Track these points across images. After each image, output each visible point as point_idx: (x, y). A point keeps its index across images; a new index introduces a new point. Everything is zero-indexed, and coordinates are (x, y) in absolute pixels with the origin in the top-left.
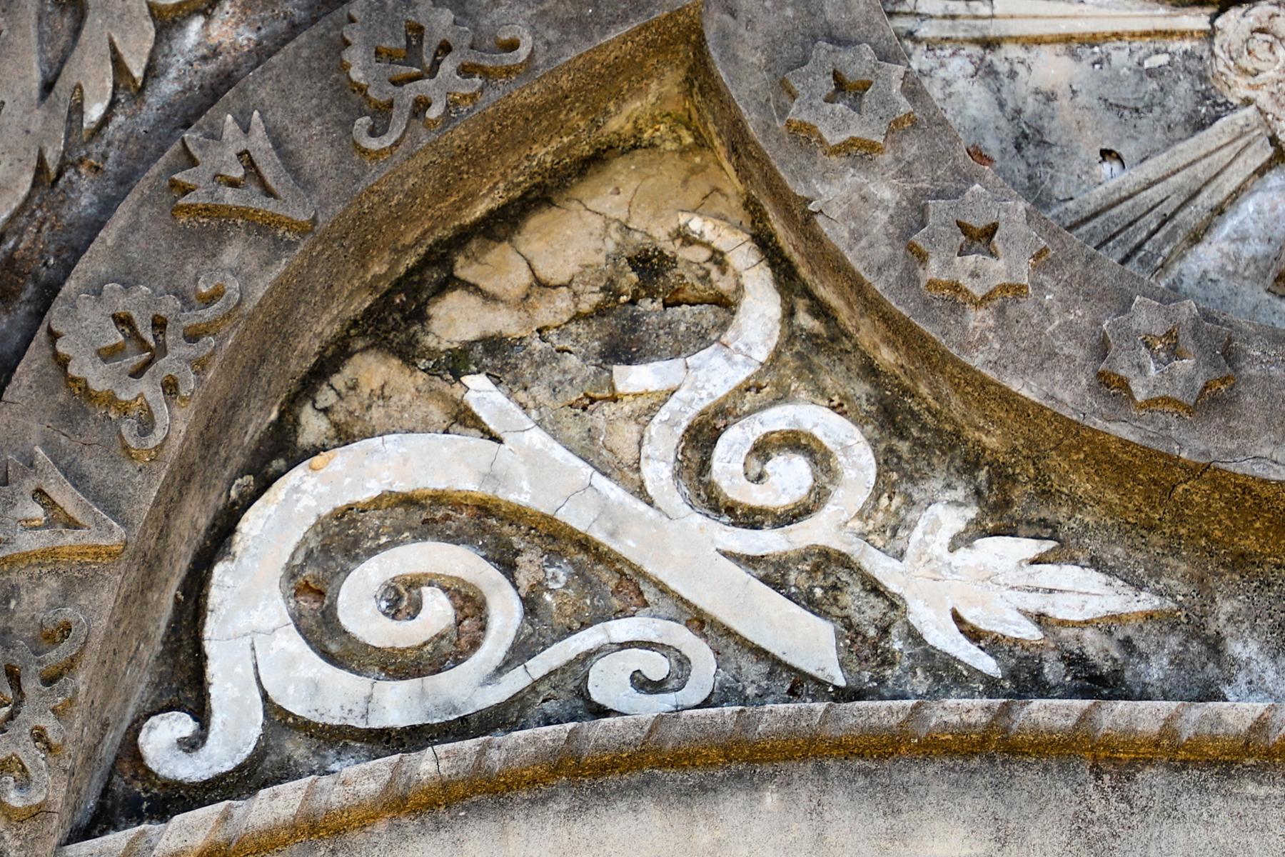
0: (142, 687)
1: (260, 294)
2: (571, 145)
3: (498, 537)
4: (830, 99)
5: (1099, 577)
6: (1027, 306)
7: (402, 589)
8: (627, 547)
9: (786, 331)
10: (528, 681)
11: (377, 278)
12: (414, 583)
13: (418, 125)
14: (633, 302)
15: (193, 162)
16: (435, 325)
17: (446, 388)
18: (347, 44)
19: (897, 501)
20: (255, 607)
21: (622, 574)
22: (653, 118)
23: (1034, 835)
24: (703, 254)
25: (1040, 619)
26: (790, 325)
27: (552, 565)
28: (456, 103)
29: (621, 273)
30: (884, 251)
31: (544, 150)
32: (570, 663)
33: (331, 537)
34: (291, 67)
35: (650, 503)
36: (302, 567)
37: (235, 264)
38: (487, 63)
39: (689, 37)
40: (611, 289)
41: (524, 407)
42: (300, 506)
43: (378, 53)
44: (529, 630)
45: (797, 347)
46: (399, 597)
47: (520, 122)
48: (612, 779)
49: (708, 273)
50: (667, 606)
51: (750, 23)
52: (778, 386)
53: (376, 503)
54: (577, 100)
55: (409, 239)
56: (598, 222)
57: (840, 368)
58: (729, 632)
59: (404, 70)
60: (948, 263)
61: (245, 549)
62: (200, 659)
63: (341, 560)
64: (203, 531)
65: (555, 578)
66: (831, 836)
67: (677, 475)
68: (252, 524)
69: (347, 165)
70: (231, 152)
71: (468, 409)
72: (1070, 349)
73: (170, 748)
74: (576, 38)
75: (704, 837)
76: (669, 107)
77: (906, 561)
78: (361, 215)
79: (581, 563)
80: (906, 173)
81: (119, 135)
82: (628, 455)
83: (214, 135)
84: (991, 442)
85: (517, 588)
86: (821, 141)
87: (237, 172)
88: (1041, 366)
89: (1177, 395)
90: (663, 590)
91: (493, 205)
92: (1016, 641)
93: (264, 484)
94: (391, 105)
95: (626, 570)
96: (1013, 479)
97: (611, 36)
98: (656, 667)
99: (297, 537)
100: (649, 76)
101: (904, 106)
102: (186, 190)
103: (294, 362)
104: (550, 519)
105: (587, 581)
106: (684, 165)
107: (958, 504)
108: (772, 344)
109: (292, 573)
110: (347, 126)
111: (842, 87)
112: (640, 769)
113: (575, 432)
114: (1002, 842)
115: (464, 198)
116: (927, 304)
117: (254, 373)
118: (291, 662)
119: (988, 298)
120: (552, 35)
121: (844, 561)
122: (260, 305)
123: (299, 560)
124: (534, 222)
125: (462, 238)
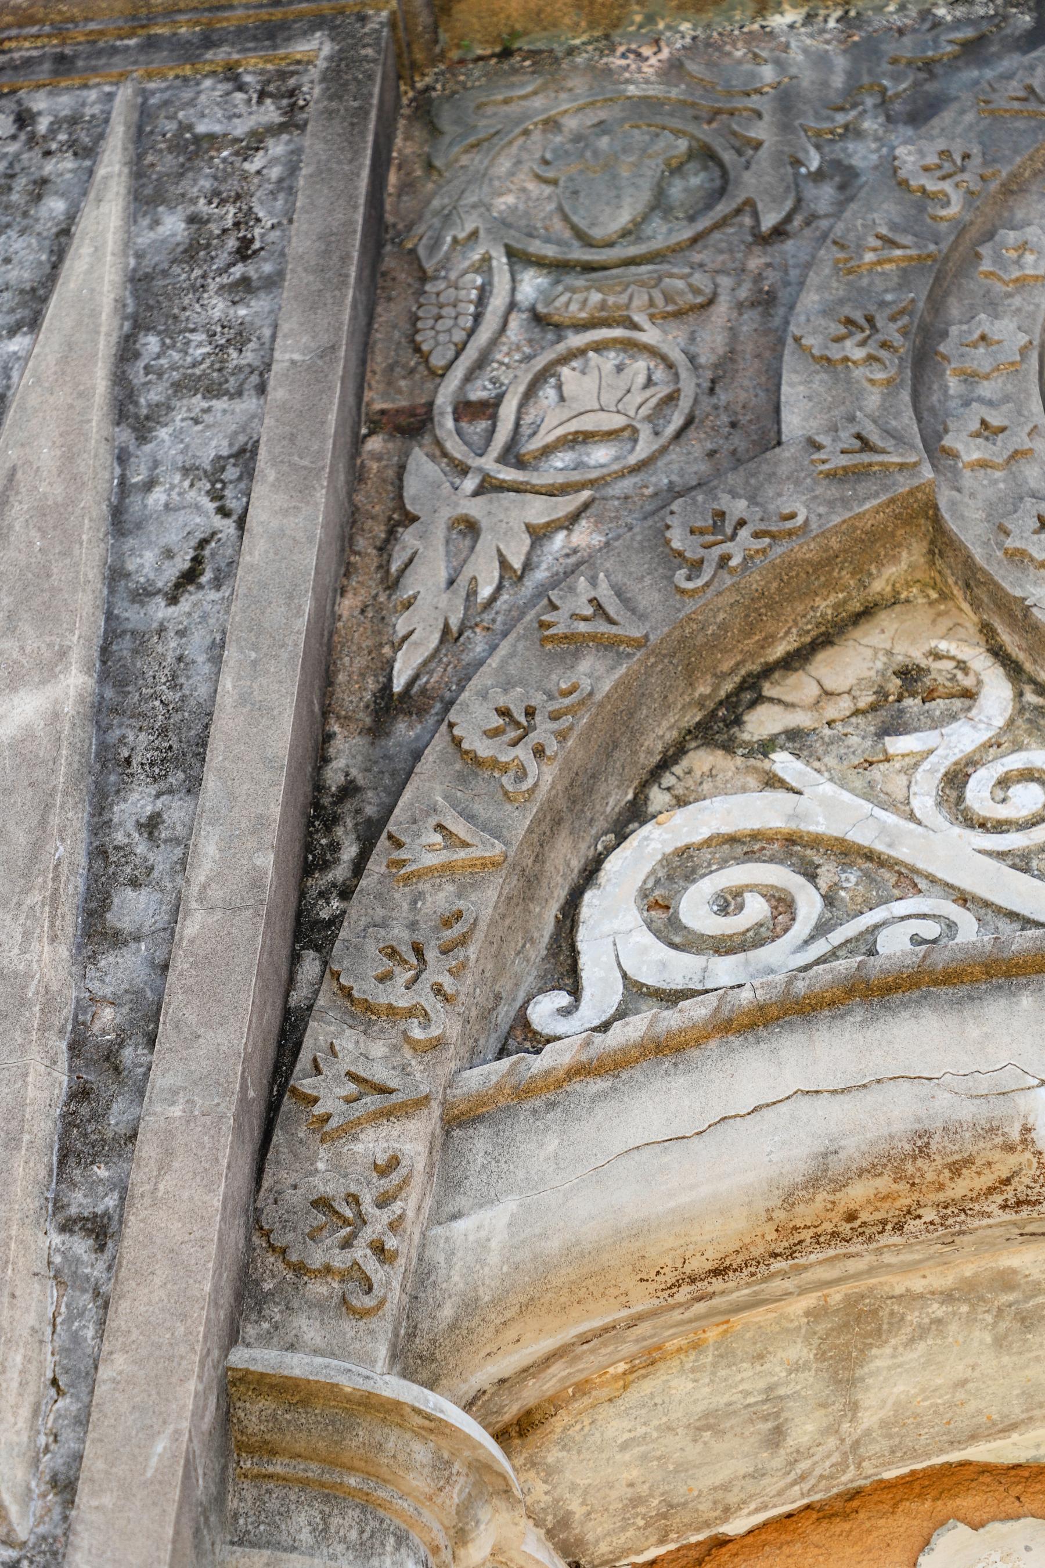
0: (530, 979)
1: (607, 688)
2: (845, 602)
3: (802, 858)
4: (1035, 532)
7: (729, 898)
8: (903, 853)
9: (1018, 706)
10: (829, 948)
11: (703, 697)
12: (738, 893)
13: (724, 574)
14: (899, 700)
15: (555, 608)
16: (750, 726)
17: (758, 764)
18: (668, 527)
21: (900, 874)
22: (907, 582)
24: (953, 664)
26: (1020, 702)
27: (845, 872)
28: (751, 557)
29: (888, 680)
31: (824, 604)
32: (862, 934)
33: (675, 869)
34: (628, 548)
35: (920, 823)
36: (653, 890)
37: (588, 671)
38: (773, 528)
39: (927, 513)
40: (882, 693)
41: (818, 771)
42: (649, 849)
43: (692, 532)
44: (828, 915)
45: (1027, 715)
46: (728, 905)
47: (803, 575)
49: (955, 676)
50: (937, 889)
51: (972, 495)
52: (1014, 742)
53: (708, 842)
54: (845, 560)
55: (726, 666)
58: (987, 904)
59: (710, 538)
61: (608, 880)
62: (574, 953)
63: (681, 883)
64: (576, 871)
65: (847, 880)
67: (939, 804)
68: (612, 865)
69: (671, 602)
70: (584, 599)
71: (775, 775)
73: (551, 1015)
74: (840, 510)
75: (974, 1032)
76: (919, 575)
78: (683, 640)
79: (868, 869)
81: (505, 607)
82: (900, 795)
83: (572, 589)
85: (818, 889)
86: (1032, 559)
87: (589, 611)
90: (933, 880)
93: (622, 837)
94: (702, 561)
95: (903, 870)
97: (867, 506)
98: (930, 930)
99: (648, 868)
100: (900, 545)
102: (550, 626)
103: (642, 755)
104: (841, 841)
105: (873, 880)
106: (932, 612)
108: (1007, 715)
110: (670, 578)
112: (919, 988)
113: (859, 784)
115: (765, 639)
117: (609, 755)
118: (644, 950)
120: (822, 510)
122: (607, 696)
123: (649, 885)
124: (821, 656)
125: (768, 671)
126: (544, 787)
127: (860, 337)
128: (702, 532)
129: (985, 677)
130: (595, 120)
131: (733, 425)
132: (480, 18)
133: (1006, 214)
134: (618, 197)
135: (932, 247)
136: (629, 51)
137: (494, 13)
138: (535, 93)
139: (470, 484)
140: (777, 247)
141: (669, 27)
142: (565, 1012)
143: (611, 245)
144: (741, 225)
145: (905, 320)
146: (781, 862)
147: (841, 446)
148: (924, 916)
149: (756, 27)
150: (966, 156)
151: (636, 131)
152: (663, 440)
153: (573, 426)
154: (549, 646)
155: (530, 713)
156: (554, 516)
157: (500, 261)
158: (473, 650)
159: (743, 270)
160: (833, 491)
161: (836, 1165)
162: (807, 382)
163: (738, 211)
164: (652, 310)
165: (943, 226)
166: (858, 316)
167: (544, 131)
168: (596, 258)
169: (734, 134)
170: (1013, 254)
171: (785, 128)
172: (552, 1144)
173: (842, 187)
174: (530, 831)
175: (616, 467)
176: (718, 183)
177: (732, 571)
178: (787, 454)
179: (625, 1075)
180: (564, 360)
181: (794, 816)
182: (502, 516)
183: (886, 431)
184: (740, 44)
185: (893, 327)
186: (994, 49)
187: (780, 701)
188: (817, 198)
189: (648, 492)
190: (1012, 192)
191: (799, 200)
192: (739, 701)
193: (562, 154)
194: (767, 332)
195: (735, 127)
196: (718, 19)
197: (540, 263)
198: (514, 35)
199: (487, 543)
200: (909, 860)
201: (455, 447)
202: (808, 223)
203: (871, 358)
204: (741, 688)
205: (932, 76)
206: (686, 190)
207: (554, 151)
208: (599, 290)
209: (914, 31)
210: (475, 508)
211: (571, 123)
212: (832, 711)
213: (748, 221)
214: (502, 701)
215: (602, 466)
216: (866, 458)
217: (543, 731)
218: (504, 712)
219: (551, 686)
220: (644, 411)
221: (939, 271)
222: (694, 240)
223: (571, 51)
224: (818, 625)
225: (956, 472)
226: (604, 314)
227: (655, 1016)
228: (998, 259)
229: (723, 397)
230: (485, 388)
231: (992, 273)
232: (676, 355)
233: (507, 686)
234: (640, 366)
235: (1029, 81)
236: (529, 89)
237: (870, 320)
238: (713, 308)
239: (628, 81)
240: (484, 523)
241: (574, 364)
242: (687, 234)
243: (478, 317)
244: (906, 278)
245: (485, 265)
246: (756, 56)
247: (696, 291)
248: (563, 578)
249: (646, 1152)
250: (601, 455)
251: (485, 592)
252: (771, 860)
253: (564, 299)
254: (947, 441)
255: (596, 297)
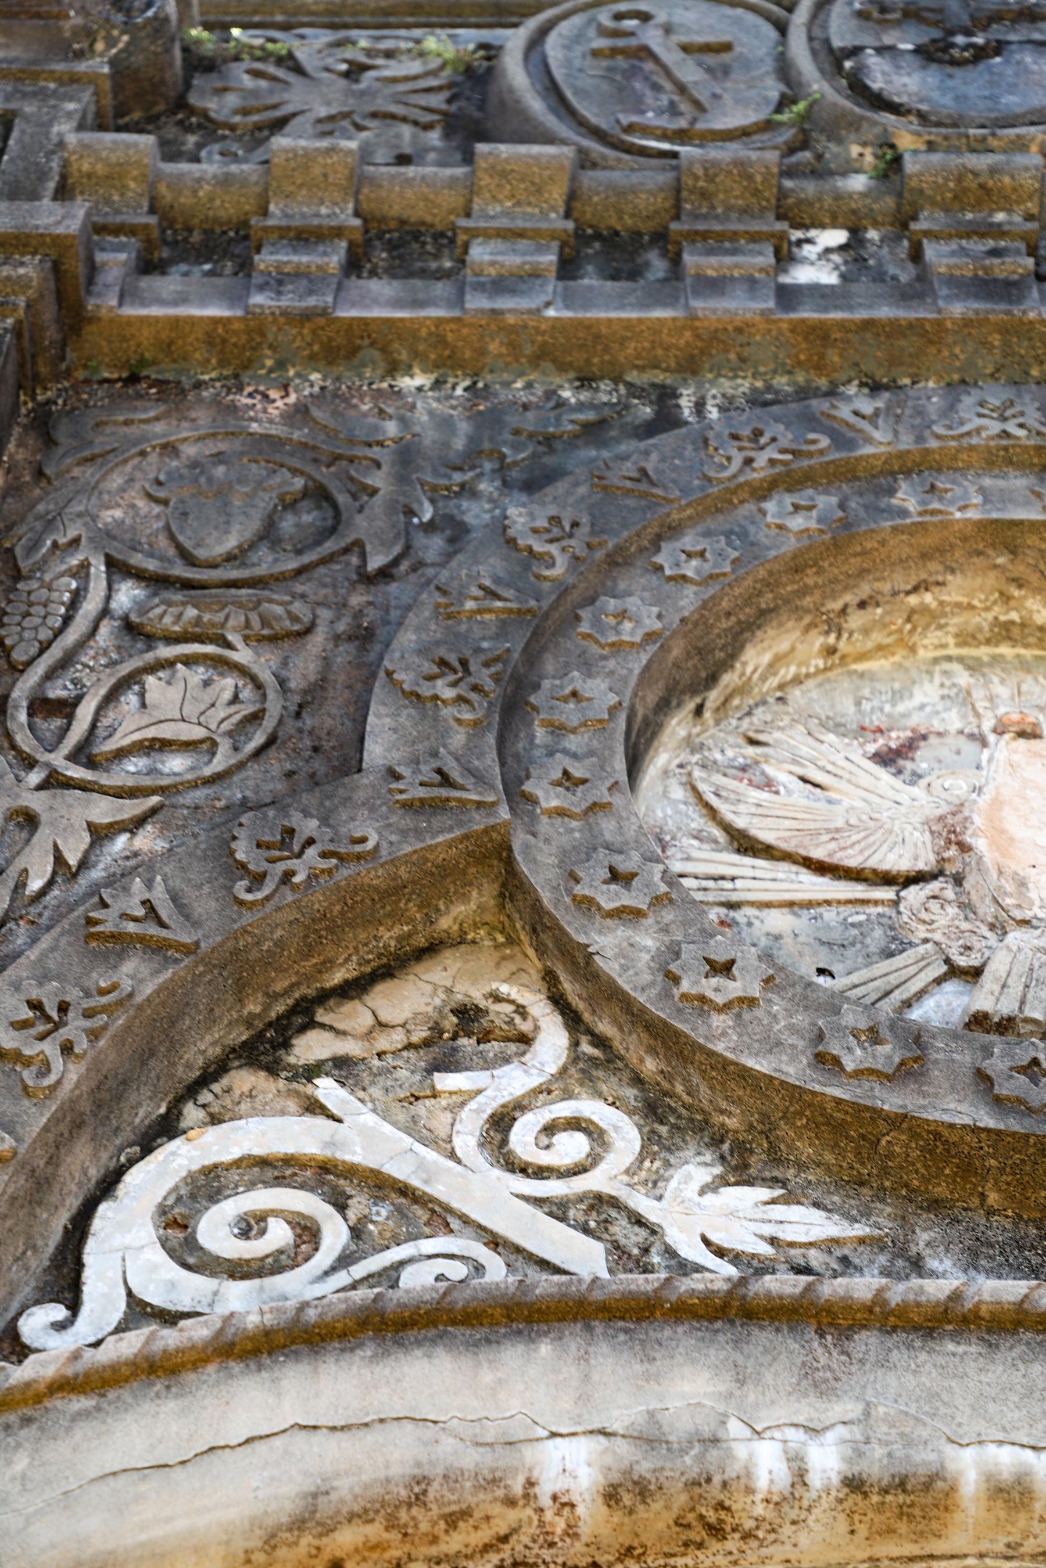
0: (28, 1289)
1: (149, 991)
2: (410, 935)
3: (334, 1188)
4: (605, 882)
5: (823, 1214)
6: (759, 1013)
8: (438, 1190)
13: (286, 890)
15: (104, 905)
16: (296, 1051)
17: (300, 1088)
18: (234, 838)
19: (657, 1164)
20: (129, 1231)
21: (433, 1211)
23: (769, 1377)
25: (773, 1241)
28: (316, 876)
29: (445, 1017)
30: (647, 977)
31: (388, 935)
32: (386, 1269)
33: (199, 1188)
35: (459, 1162)
40: (437, 1029)
41: (361, 1101)
42: (175, 1165)
44: (354, 1247)
45: (581, 1065)
46: (250, 1228)
47: (368, 902)
48: (412, 1334)
50: (469, 1231)
51: (547, 841)
53: (237, 1163)
55: (279, 986)
56: (429, 988)
57: (614, 1080)
58: (518, 1250)
59: (277, 853)
60: (696, 983)
62: (79, 1266)
64: (93, 1181)
65: (378, 1214)
66: (596, 1377)
67: (481, 1145)
68: (133, 1178)
69: (228, 912)
70: (136, 900)
71: (317, 1101)
72: (793, 1040)
73: (45, 1328)
75: (487, 1377)
76: (488, 917)
77: (664, 1201)
78: (236, 952)
80: (665, 930)
82: (443, 1133)
83: (126, 889)
84: (732, 1123)
85: (346, 1220)
86: (599, 908)
87: (140, 912)
88: (770, 1051)
89: (879, 1067)
90: (466, 1220)
91: (348, 976)
92: (753, 1256)
93: (147, 1150)
94: (264, 875)
96: (751, 1151)
97: (440, 839)
98: (457, 1271)
99: (170, 1184)
100: (471, 884)
101: (663, 888)
103: (181, 1069)
104: (376, 1173)
106: (497, 955)
107: (706, 1164)
109: (163, 1210)
110: (229, 889)
111: (615, 876)
112: (436, 1326)
114: (741, 1382)
115: (324, 963)
116: (679, 1011)
117: (144, 1063)
118: (154, 1268)
119: (727, 1007)
120: (394, 838)
121: (614, 1202)
122: (148, 1000)
123: (170, 1201)
124: (380, 988)
125: (324, 997)
126: (68, 1086)
127: (452, 678)
128: (269, 846)
129: (542, 1024)
130: (215, 451)
131: (316, 749)
132: (110, 342)
133: (609, 583)
134: (228, 523)
135: (532, 603)
136: (256, 391)
137: (124, 339)
138: (157, 419)
139: (35, 778)
140: (381, 587)
141: (298, 375)
142: (60, 1326)
143: (214, 566)
144: (348, 564)
145: (499, 667)
146: (312, 1190)
147: (421, 778)
148: (452, 1257)
149: (385, 385)
150: (575, 525)
151: (254, 466)
152: (240, 756)
153: (151, 733)
154: (94, 944)
155: (63, 1008)
156: (119, 818)
157: (99, 568)
158: (13, 942)
159: (344, 605)
160: (408, 821)
161: (325, 1507)
162: (395, 715)
163: (346, 550)
164: (247, 632)
165: (546, 586)
166: (453, 659)
167: (161, 455)
168: (198, 576)
169: (352, 479)
170: (612, 621)
171: (402, 479)
172: (21, 1462)
173: (452, 540)
174: (46, 1129)
175: (189, 777)
176: (330, 522)
177: (295, 888)
178: (365, 781)
179: (112, 1395)
180: (152, 669)
181: (331, 1144)
182: (64, 812)
183: (469, 771)
184: (367, 399)
185: (486, 672)
186: (613, 433)
187: (331, 1028)
188: (426, 547)
189: (218, 804)
190: (617, 564)
191: (408, 548)
192: (290, 1024)
193: (175, 477)
194: (360, 666)
195: (353, 473)
196: (347, 374)
197: (139, 575)
198: (143, 362)
199: (43, 837)
200: (443, 1198)
201: (24, 740)
202: (414, 569)
203: (461, 699)
204: (293, 1011)
205: (551, 450)
206: (297, 525)
207: (169, 474)
208: (195, 606)
209: (538, 407)
210: (37, 802)
211: (190, 451)
212: (383, 1042)
213: (355, 560)
214: (35, 994)
215: (175, 774)
216: (444, 792)
217: (75, 1028)
218: (36, 1006)
219: (89, 984)
220: (226, 726)
221: (538, 626)
222: (299, 572)
223: (198, 385)
224: (380, 956)
225: (533, 818)
226: (198, 630)
227: (153, 1334)
228: (597, 623)
229: (308, 721)
230: (65, 688)
231: (589, 636)
232: (266, 676)
233: (43, 979)
234: (228, 684)
235: (643, 464)
236: (152, 414)
237: (464, 663)
238: (309, 637)
239: (252, 419)
240: (44, 818)
241: (161, 674)
242: (293, 564)
243: (67, 620)
244: (503, 630)
245: (82, 571)
246: (381, 411)
247: (294, 619)
248: (118, 880)
249: (123, 1479)
250: (176, 764)
251: (35, 885)
252: (302, 1187)
253: (158, 611)
254: (528, 787)
255: (191, 612)
